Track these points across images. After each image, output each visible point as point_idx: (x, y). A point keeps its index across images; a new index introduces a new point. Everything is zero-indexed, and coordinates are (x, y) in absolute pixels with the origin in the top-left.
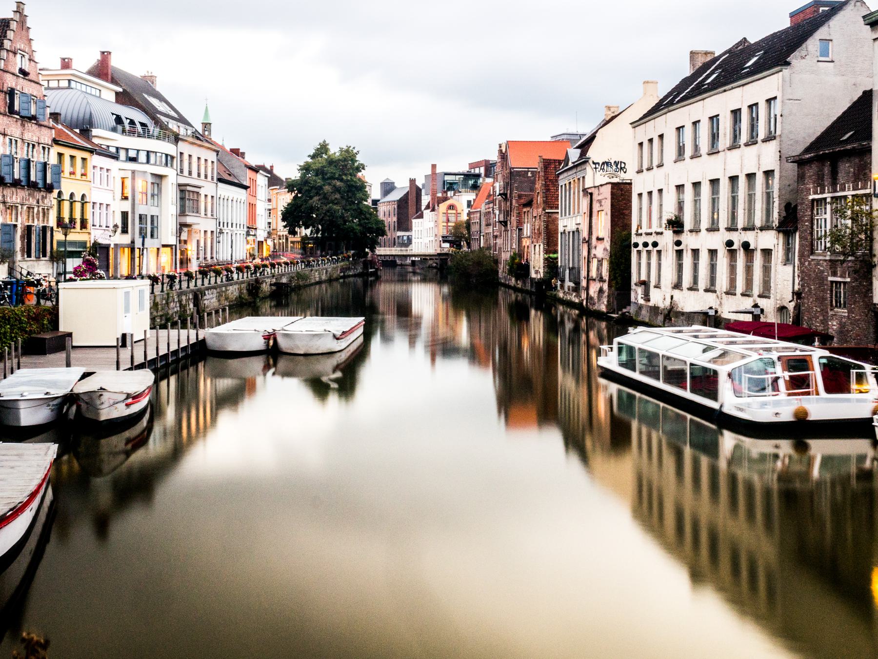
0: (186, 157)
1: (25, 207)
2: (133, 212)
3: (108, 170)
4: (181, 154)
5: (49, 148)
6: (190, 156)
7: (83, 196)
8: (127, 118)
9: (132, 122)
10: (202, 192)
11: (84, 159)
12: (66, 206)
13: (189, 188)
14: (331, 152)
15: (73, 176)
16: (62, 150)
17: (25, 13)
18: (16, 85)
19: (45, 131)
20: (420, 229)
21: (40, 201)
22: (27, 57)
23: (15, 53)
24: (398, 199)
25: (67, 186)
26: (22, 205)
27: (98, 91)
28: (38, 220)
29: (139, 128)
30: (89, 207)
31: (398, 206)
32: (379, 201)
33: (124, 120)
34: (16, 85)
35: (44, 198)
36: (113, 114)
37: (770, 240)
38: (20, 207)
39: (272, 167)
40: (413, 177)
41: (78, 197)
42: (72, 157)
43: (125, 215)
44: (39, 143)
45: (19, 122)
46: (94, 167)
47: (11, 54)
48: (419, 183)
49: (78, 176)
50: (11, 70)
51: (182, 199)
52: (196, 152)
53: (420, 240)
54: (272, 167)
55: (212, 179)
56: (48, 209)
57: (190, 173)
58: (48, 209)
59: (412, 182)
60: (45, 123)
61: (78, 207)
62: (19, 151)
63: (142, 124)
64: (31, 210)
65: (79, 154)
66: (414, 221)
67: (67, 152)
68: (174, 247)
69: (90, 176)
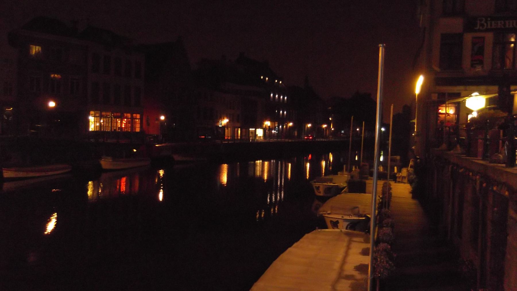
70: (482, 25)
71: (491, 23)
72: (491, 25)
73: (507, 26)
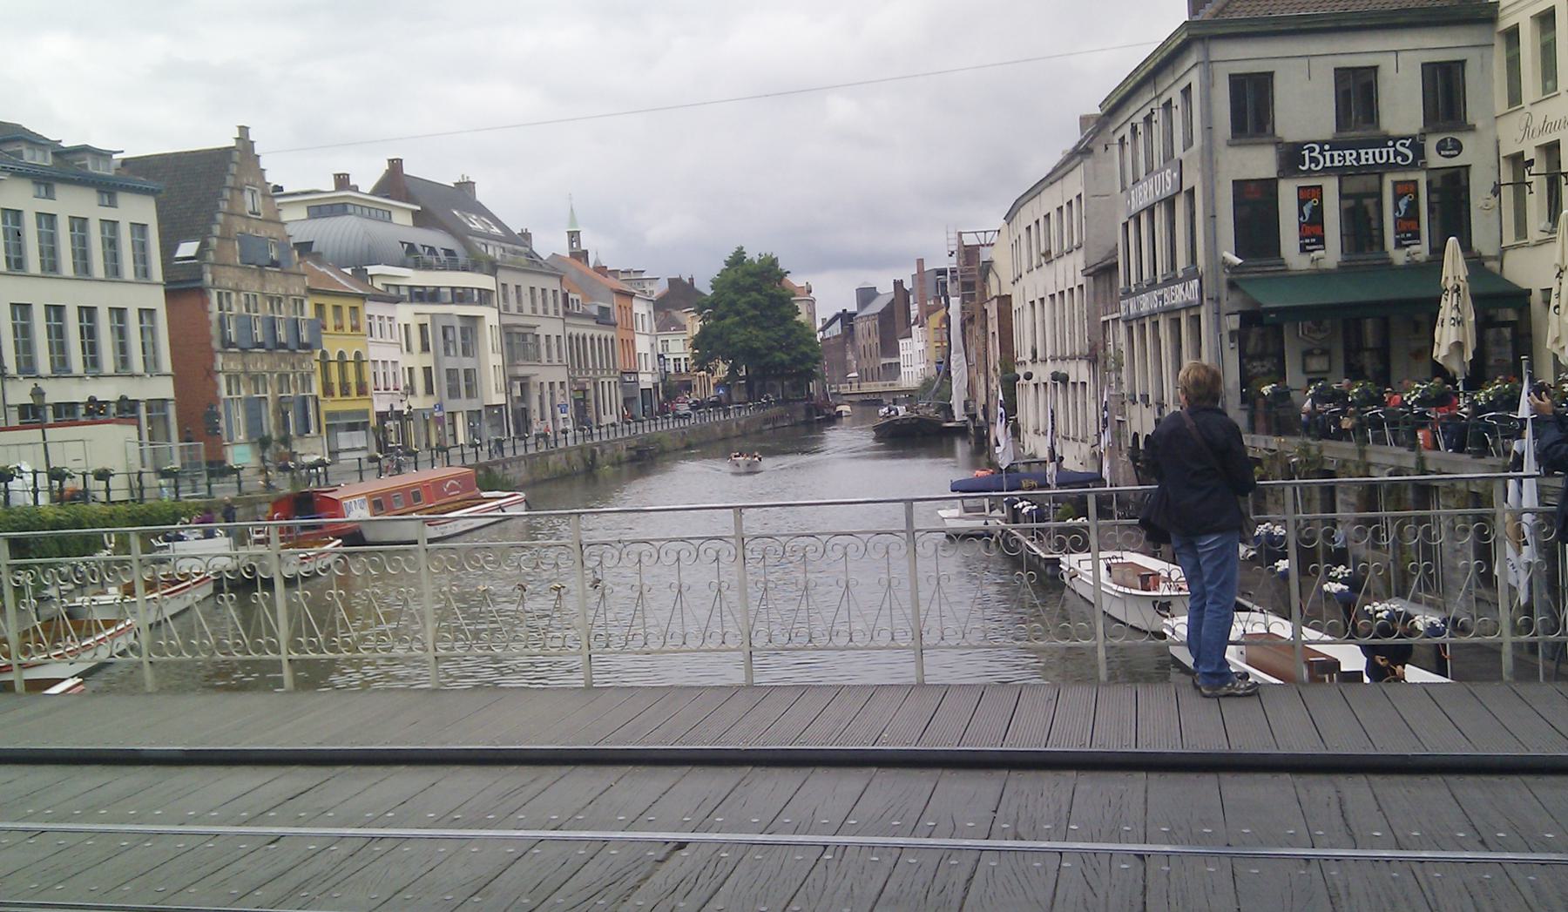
0: (511, 288)
1: (275, 375)
2: (437, 368)
3: (390, 319)
4: (504, 285)
5: (302, 302)
6: (518, 287)
7: (358, 354)
8: (424, 246)
9: (432, 250)
10: (540, 331)
11: (354, 309)
12: (334, 368)
13: (517, 330)
14: (748, 256)
15: (339, 332)
16: (320, 300)
17: (251, 139)
18: (248, 229)
19: (294, 280)
20: (909, 352)
21: (296, 365)
22: (259, 192)
23: (242, 191)
24: (879, 311)
25: (333, 345)
26: (271, 373)
27: (387, 214)
28: (296, 388)
29: (443, 257)
30: (368, 370)
31: (881, 323)
32: (855, 314)
33: (420, 249)
34: (248, 229)
35: (301, 361)
36: (403, 243)
37: (1079, 371)
38: (268, 375)
39: (691, 279)
40: (898, 279)
41: (350, 356)
42: (337, 308)
43: (427, 371)
44: (287, 296)
45: (256, 274)
46: (370, 317)
47: (236, 193)
48: (908, 285)
49: (348, 329)
50: (238, 210)
51: (510, 344)
52: (526, 282)
53: (910, 369)
54: (691, 279)
55: (556, 312)
56: (308, 375)
57: (520, 309)
58: (308, 375)
59: (898, 284)
60: (294, 269)
61: (351, 368)
62: (259, 308)
63: (449, 252)
64: (285, 380)
65: (346, 304)
66: (901, 342)
67: (329, 303)
68: (504, 407)
69: (364, 328)
70: (1313, 160)
71: (1332, 156)
72: (1332, 161)
73: (1363, 162)
